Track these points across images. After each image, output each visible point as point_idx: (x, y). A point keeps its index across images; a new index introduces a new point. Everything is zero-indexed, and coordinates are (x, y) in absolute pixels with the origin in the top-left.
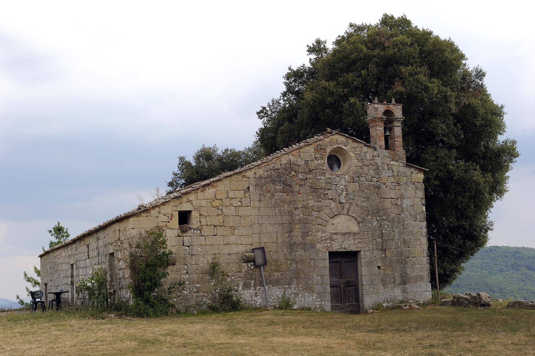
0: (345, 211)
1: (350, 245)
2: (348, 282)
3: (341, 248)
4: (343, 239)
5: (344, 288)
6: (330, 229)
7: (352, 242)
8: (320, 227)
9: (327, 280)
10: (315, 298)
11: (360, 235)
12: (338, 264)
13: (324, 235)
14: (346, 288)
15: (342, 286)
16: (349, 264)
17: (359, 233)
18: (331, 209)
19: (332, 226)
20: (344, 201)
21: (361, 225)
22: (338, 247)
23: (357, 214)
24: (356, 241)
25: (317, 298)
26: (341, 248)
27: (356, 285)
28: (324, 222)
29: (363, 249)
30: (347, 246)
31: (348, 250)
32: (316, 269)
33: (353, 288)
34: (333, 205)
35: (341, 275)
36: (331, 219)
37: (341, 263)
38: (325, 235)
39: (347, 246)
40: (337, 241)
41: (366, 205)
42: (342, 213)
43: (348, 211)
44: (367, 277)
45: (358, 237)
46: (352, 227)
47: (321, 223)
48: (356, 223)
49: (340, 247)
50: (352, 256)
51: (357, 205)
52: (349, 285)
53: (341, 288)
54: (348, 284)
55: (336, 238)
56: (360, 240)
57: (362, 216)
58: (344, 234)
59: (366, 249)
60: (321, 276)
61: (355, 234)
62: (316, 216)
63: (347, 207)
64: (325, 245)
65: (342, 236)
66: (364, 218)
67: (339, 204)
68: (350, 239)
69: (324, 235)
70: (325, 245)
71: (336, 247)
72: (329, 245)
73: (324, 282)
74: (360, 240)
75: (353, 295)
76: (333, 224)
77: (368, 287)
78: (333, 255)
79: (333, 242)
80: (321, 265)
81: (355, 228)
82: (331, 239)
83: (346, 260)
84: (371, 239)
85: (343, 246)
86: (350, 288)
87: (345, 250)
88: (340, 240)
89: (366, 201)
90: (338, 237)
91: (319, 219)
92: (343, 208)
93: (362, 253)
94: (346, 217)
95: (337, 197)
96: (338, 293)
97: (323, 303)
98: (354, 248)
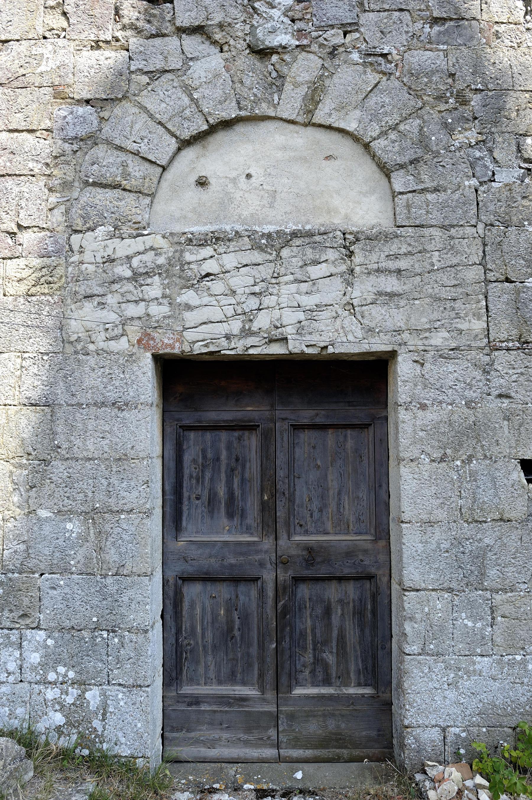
0: (290, 103)
1: (313, 316)
2: (312, 554)
3: (246, 333)
4: (265, 271)
5: (279, 590)
6: (178, 208)
7: (332, 292)
8: (103, 197)
9: (142, 537)
10: (35, 658)
11: (394, 247)
12: (253, 441)
13: (123, 248)
14: (304, 591)
15: (268, 576)
16: (331, 438)
17: (384, 237)
18: (188, 90)
19: (192, 195)
20: (284, 38)
21: (400, 181)
22: (222, 329)
23: (375, 117)
24: (363, 290)
25: (51, 661)
26: (246, 333)
27: (370, 577)
28: (137, 170)
29: (414, 342)
30: (290, 317)
31: (296, 346)
32: (59, 469)
33: (351, 590)
34: (208, 63)
35: (268, 510)
36: (189, 154)
37: (268, 438)
38: (138, 244)
39: (290, 317)
40: (217, 287)
41: (441, 62)
42: (264, 109)
43: (314, 96)
44: (438, 534)
45: (377, 257)
46: (336, 202)
47: (113, 173)
48: (368, 169)
49: (236, 326)
50: (346, 388)
51: (374, 57)
52: (323, 571)
53: (262, 592)
54: (313, 567)
55: (211, 266)
56: (391, 284)
57: (412, 126)
58: (274, 243)
59: (439, 339)
60: (91, 514)
61: (350, 243)
62: (82, 131)
63: (305, 77)
64: (132, 310)
65: (257, 257)
66: (423, 141)
67: (245, 61)
68: (315, 271)
69: (123, 248)
70: (132, 310)
71: (209, 327)
72: (158, 311)
73: (112, 556)
74: (391, 284)
75: (352, 635)
76: (202, 183)
77: (440, 603)
78: (185, 379)
79: (189, 296)
80: (91, 446)
81: (356, 200)
82: (178, 274)
83: (306, 415)
84: (474, 274)
85: (262, 321)
86: (333, 592)
87: (277, 349)
88: (241, 281)
89: (443, 38)
90: (230, 261)
91: (100, 151)
92: (277, 83)
93: (404, 368)
94: (301, 139)
95: (236, 13)
96: (245, 618)
97: (93, 696)
98: (345, 337)
